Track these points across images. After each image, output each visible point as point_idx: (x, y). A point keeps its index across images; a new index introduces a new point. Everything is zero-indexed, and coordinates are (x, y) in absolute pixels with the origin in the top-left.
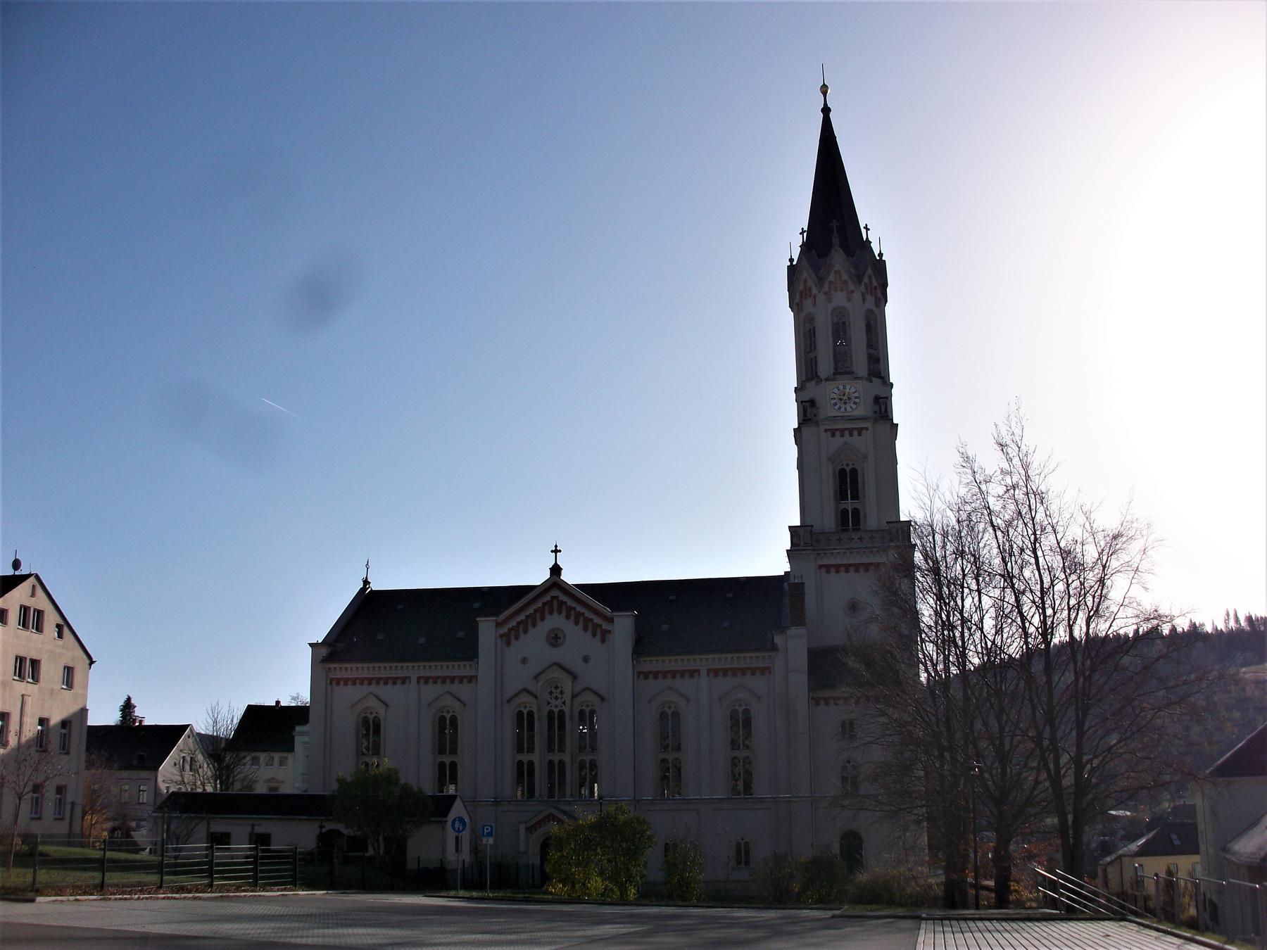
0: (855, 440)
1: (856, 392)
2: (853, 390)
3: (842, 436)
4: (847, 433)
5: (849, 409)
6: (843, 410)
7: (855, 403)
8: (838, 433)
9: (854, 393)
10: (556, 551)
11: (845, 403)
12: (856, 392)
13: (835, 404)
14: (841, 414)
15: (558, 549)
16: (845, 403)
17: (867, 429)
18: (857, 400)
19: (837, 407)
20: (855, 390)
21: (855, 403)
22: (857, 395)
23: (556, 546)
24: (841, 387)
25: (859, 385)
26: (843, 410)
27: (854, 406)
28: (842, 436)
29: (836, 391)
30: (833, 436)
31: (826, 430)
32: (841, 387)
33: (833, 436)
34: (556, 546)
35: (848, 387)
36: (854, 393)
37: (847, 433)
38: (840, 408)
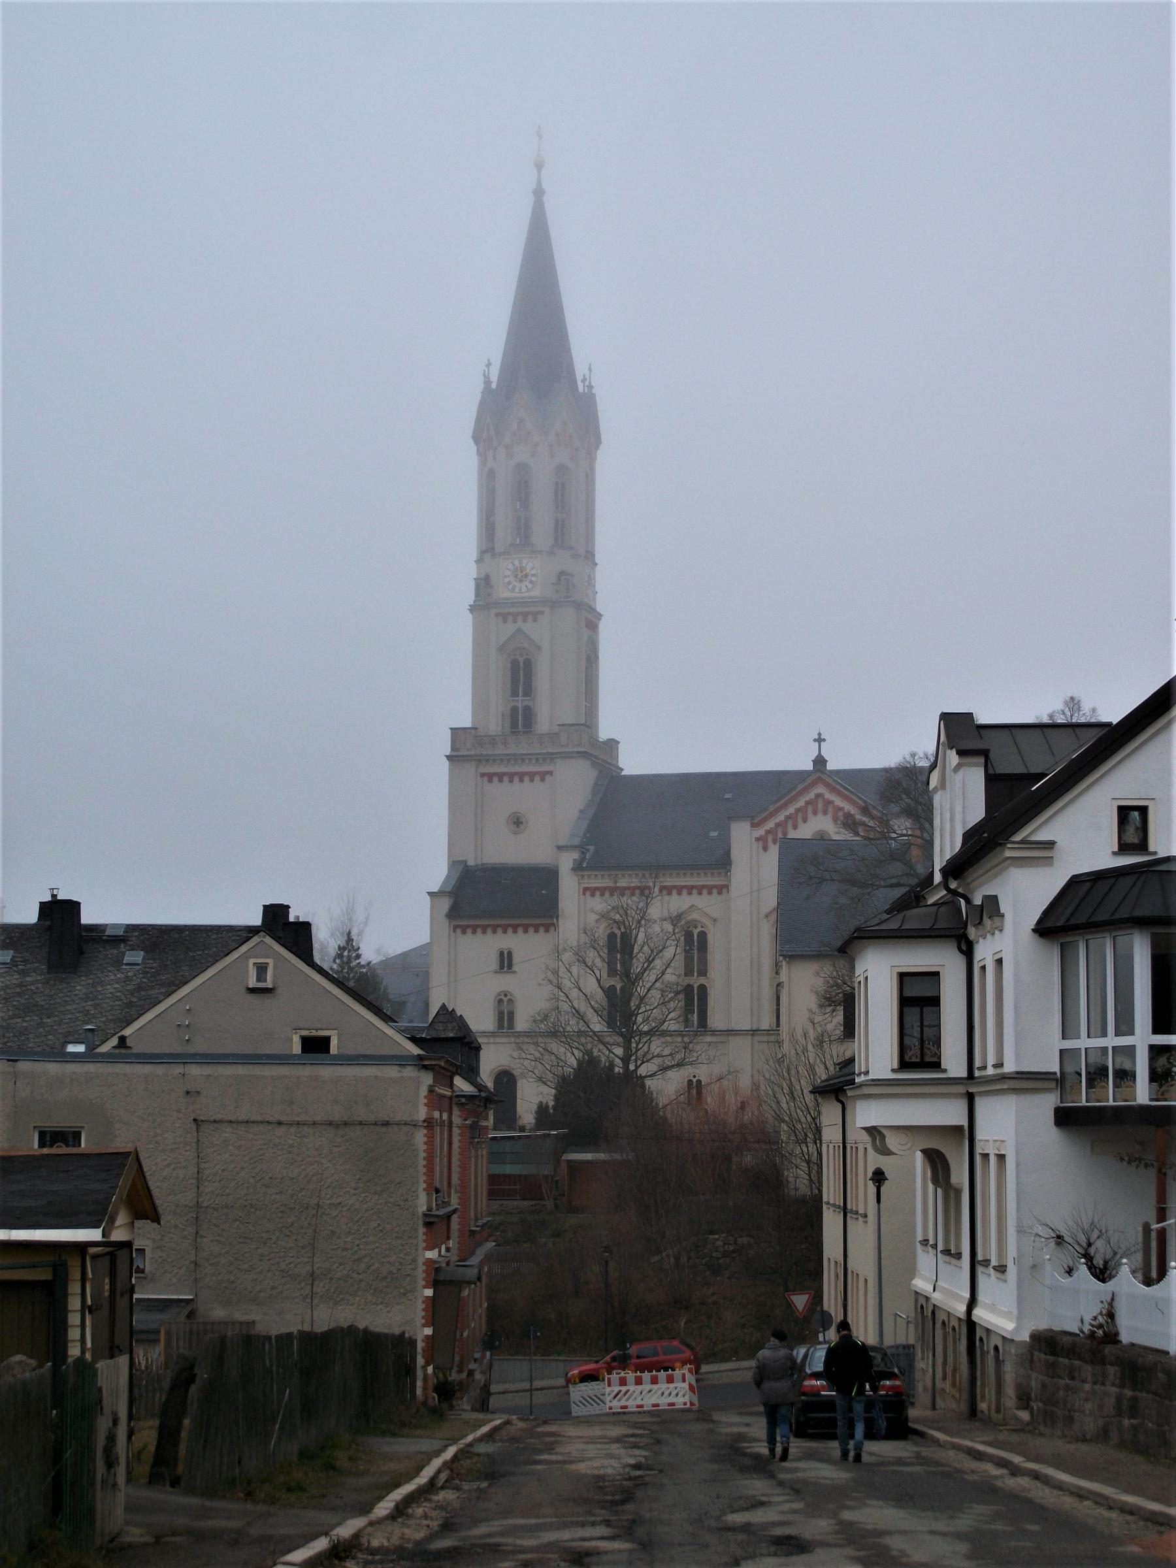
0: (528, 627)
1: (532, 568)
2: (531, 565)
3: (515, 621)
4: (520, 619)
5: (524, 589)
7: (531, 582)
8: (510, 619)
10: (820, 740)
12: (532, 568)
13: (509, 583)
14: (518, 595)
17: (542, 613)
18: (534, 579)
21: (531, 582)
23: (819, 734)
24: (517, 563)
27: (530, 586)
28: (515, 621)
29: (511, 566)
30: (505, 621)
31: (497, 615)
33: (505, 621)
34: (819, 734)
35: (525, 562)
37: (520, 619)
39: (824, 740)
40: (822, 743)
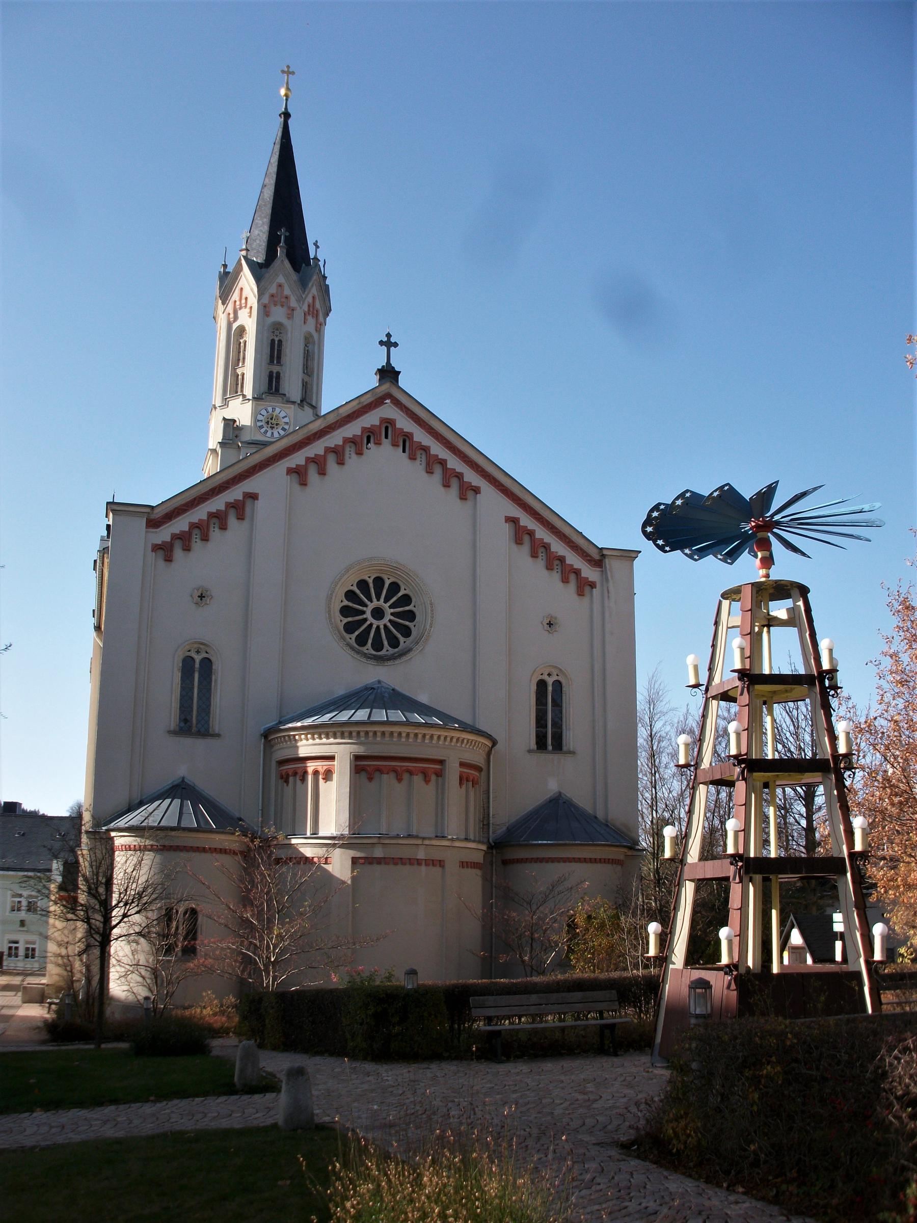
1: (286, 417)
2: (283, 414)
6: (269, 434)
9: (283, 418)
10: (389, 344)
11: (272, 428)
12: (286, 417)
13: (261, 427)
15: (393, 340)
16: (272, 428)
19: (263, 430)
20: (285, 415)
22: (286, 420)
23: (389, 335)
24: (270, 409)
25: (291, 410)
26: (269, 434)
29: (264, 412)
32: (270, 409)
34: (389, 335)
35: (278, 410)
36: (283, 418)
38: (266, 432)
39: (396, 345)
40: (392, 349)
